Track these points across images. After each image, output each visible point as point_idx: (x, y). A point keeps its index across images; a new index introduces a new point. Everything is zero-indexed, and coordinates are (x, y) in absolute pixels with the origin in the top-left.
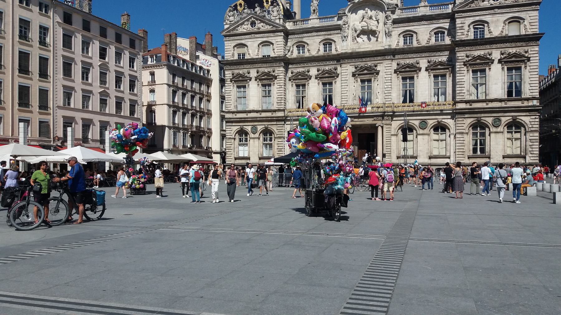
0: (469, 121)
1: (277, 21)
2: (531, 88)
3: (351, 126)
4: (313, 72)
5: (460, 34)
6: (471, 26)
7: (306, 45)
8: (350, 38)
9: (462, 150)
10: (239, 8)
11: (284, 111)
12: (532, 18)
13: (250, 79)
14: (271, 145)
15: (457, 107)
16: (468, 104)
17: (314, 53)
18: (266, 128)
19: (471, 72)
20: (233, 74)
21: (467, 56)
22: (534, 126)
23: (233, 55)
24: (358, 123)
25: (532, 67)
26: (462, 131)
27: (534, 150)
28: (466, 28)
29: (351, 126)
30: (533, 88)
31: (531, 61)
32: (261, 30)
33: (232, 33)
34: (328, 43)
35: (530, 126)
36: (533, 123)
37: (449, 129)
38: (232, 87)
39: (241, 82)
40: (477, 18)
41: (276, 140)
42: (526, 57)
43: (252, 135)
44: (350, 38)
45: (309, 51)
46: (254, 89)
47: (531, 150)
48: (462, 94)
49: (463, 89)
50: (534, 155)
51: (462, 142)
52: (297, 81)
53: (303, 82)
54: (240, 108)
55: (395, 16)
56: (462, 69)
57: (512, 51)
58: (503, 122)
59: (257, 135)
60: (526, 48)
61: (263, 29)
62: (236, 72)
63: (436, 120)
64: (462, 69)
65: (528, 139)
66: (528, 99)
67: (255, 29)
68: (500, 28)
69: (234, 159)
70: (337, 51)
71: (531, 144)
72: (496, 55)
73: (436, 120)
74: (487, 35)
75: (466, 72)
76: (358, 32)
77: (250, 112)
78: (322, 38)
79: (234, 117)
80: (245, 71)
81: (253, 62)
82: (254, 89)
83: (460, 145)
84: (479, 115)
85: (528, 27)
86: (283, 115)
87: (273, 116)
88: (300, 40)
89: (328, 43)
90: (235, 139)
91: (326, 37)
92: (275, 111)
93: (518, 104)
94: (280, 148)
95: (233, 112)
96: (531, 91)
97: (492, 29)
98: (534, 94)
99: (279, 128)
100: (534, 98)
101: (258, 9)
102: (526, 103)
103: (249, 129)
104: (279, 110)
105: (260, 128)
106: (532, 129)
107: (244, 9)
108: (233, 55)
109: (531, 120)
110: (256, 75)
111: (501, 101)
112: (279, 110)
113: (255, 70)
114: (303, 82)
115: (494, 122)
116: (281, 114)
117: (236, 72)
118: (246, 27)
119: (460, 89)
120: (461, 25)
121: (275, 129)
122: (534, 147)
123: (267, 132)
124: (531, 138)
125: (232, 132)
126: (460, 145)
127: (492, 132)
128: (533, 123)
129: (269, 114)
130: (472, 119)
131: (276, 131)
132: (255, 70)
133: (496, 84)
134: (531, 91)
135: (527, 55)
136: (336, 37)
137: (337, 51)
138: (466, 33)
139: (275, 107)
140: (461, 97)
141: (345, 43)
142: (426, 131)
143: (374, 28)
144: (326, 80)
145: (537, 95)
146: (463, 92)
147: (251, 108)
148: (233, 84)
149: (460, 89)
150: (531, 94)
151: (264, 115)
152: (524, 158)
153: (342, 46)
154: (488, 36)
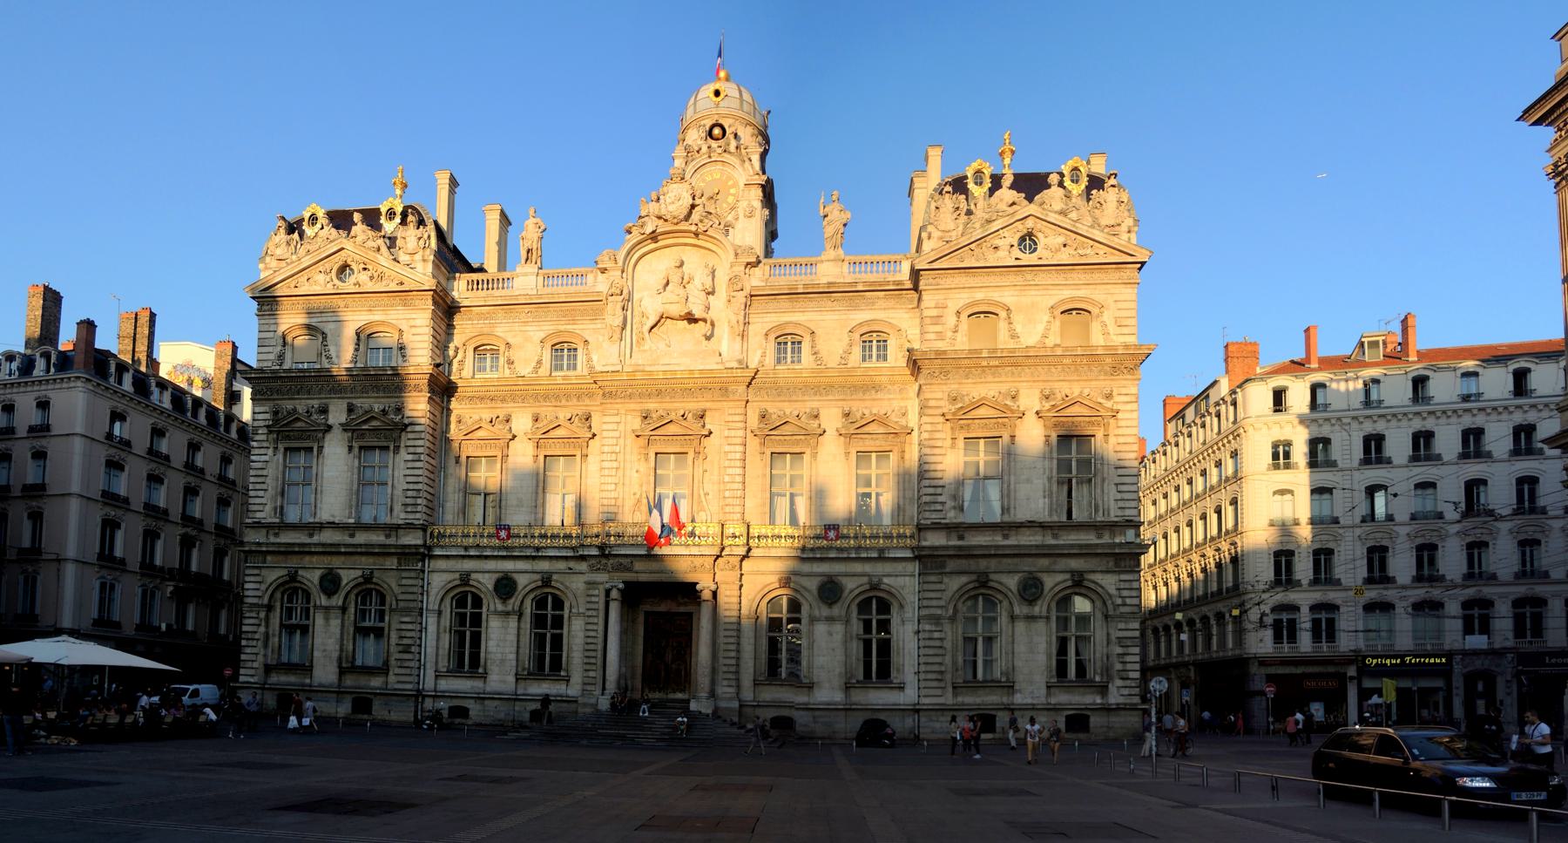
0: (954, 584)
2: (1119, 496)
3: (621, 586)
5: (932, 336)
6: (964, 316)
9: (936, 668)
11: (424, 528)
12: (1120, 305)
13: (330, 428)
14: (379, 633)
15: (924, 543)
16: (954, 535)
18: (368, 579)
19: (961, 443)
20: (276, 413)
22: (1128, 601)
24: (643, 578)
25: (1121, 440)
26: (939, 612)
27: (1129, 667)
28: (951, 320)
29: (621, 586)
30: (1126, 496)
31: (1122, 423)
35: (1119, 601)
36: (1125, 593)
37: (902, 606)
38: (270, 452)
39: (296, 437)
40: (979, 295)
41: (396, 618)
42: (1108, 409)
43: (324, 601)
46: (336, 461)
47: (1119, 666)
48: (939, 507)
49: (939, 491)
50: (1128, 683)
51: (938, 643)
54: (293, 516)
56: (938, 435)
58: (1047, 588)
59: (338, 600)
60: (1105, 384)
62: (288, 405)
63: (865, 579)
64: (938, 435)
65: (1113, 638)
68: (1040, 328)
69: (262, 671)
71: (1119, 650)
73: (865, 579)
74: (1004, 341)
75: (949, 442)
77: (321, 526)
79: (272, 539)
80: (316, 403)
82: (336, 461)
83: (931, 652)
84: (983, 564)
86: (420, 542)
87: (388, 542)
90: (269, 608)
92: (393, 529)
94: (405, 641)
95: (269, 527)
96: (1121, 504)
97: (1019, 329)
98: (1128, 512)
99: (404, 582)
102: (1106, 539)
103: (312, 577)
105: (348, 576)
106: (1123, 609)
109: (1122, 585)
110: (343, 418)
111: (1042, 526)
112: (410, 527)
115: (1025, 589)
116: (412, 539)
117: (288, 405)
119: (931, 491)
120: (934, 313)
121: (394, 585)
122: (1128, 659)
123: (368, 590)
124: (1121, 634)
125: (263, 587)
126: (931, 652)
127: (1018, 617)
128: (1125, 593)
129: (377, 538)
130: (964, 579)
133: (1028, 481)
134: (1121, 504)
135: (1108, 404)
138: (950, 334)
139: (400, 517)
140: (934, 516)
142: (836, 610)
146: (940, 499)
147: (324, 515)
148: (276, 441)
149: (931, 491)
150: (1120, 513)
151: (361, 538)
152: (1103, 689)
154: (1012, 345)
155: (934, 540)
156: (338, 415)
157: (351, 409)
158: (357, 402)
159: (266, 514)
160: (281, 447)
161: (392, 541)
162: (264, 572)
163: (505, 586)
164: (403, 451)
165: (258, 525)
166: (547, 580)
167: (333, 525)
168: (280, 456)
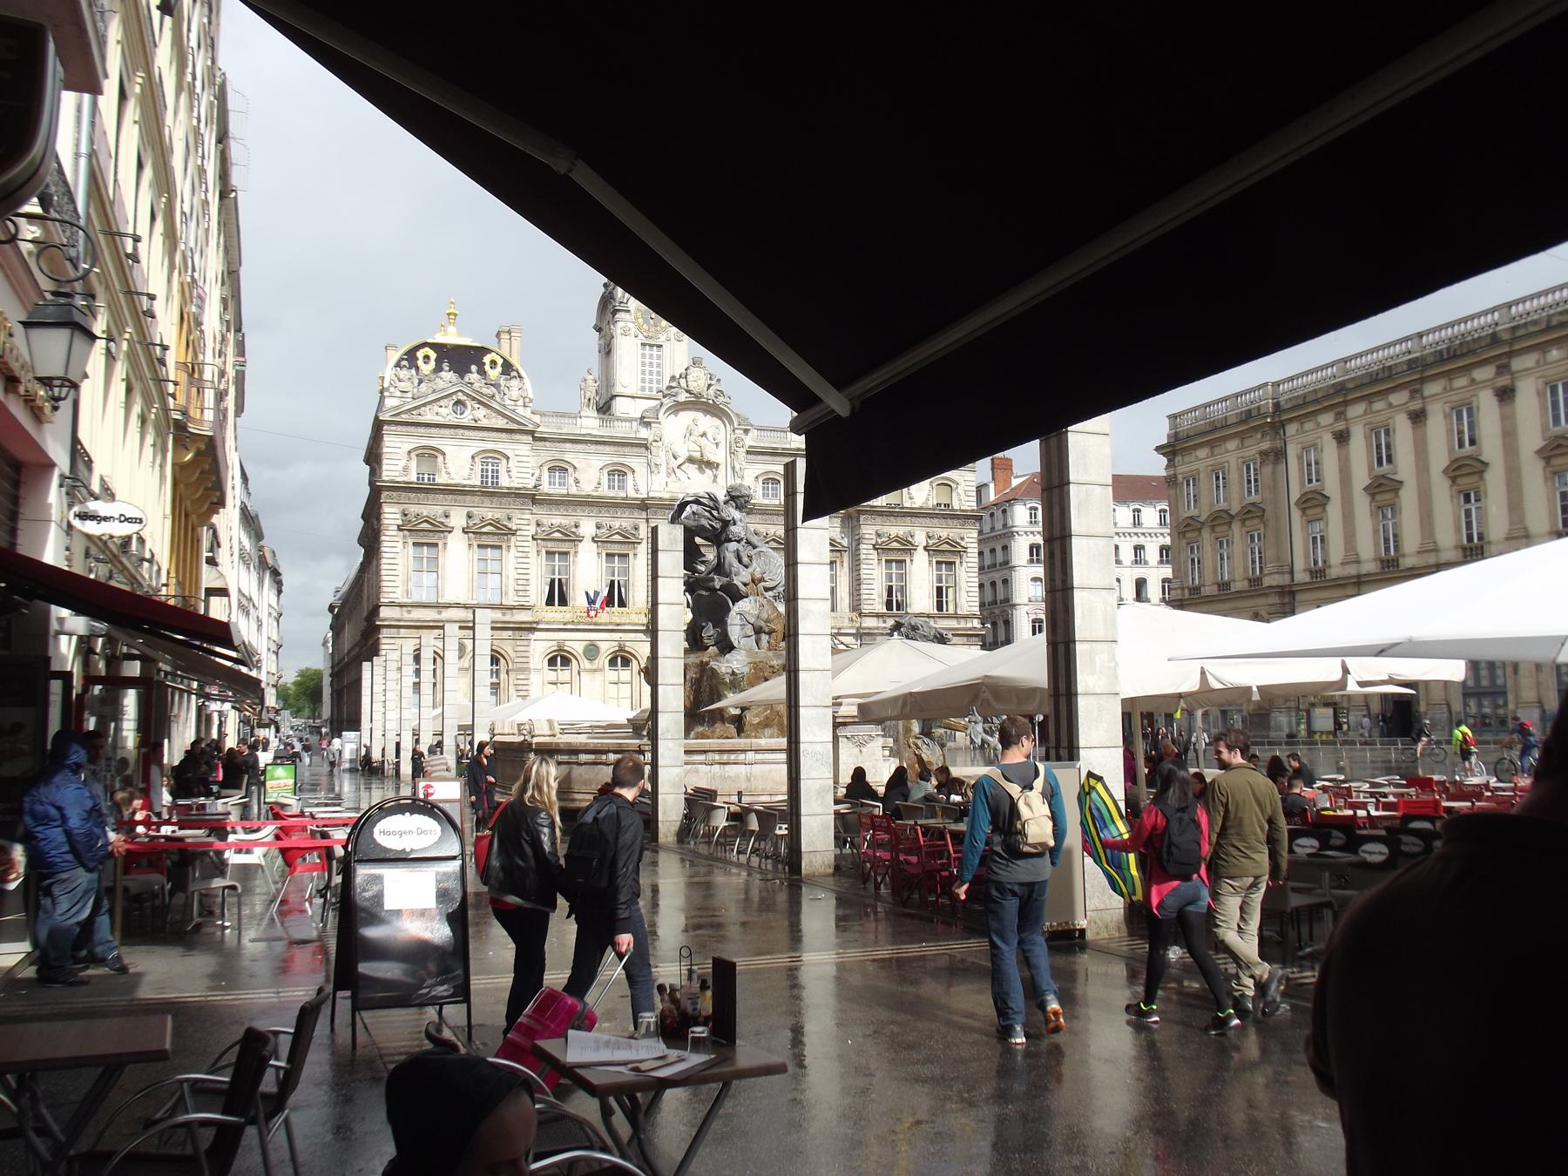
1: (520, 410)
4: (587, 527)
7: (570, 470)
8: (663, 469)
10: (420, 363)
17: (587, 488)
21: (878, 535)
23: (406, 469)
32: (479, 424)
33: (405, 417)
34: (618, 473)
38: (400, 545)
44: (663, 469)
45: (577, 482)
52: (549, 544)
53: (563, 547)
55: (750, 440)
57: (944, 533)
61: (484, 423)
62: (413, 509)
66: (965, 617)
67: (466, 419)
68: (925, 493)
70: (637, 491)
72: (920, 538)
76: (680, 461)
77: (448, 606)
78: (608, 460)
79: (406, 616)
80: (439, 510)
81: (456, 492)
85: (962, 496)
88: (558, 456)
89: (618, 473)
91: (616, 460)
92: (512, 608)
93: (953, 623)
100: (973, 616)
101: (473, 376)
102: (963, 625)
104: (523, 608)
107: (438, 369)
108: (406, 469)
112: (523, 608)
113: (465, 511)
114: (563, 547)
118: (445, 413)
131: (513, 655)
132: (465, 511)
136: (636, 462)
137: (637, 491)
139: (511, 600)
141: (656, 478)
143: (713, 458)
144: (616, 549)
145: (976, 610)
147: (448, 598)
153: (647, 482)
155: (870, 623)
156: (458, 519)
157: (469, 516)
158: (475, 511)
159: (399, 596)
160: (410, 542)
161: (508, 618)
162: (399, 641)
163: (592, 651)
164: (513, 549)
165: (392, 604)
166: (621, 649)
167: (457, 605)
168: (411, 548)
